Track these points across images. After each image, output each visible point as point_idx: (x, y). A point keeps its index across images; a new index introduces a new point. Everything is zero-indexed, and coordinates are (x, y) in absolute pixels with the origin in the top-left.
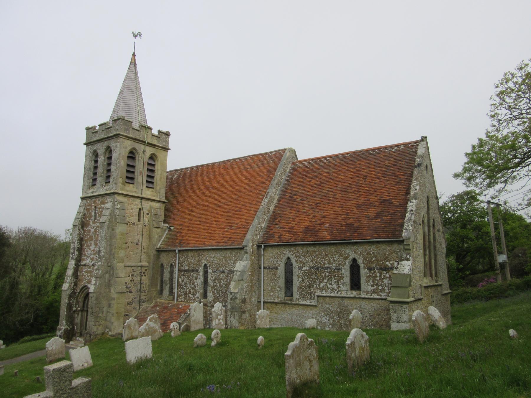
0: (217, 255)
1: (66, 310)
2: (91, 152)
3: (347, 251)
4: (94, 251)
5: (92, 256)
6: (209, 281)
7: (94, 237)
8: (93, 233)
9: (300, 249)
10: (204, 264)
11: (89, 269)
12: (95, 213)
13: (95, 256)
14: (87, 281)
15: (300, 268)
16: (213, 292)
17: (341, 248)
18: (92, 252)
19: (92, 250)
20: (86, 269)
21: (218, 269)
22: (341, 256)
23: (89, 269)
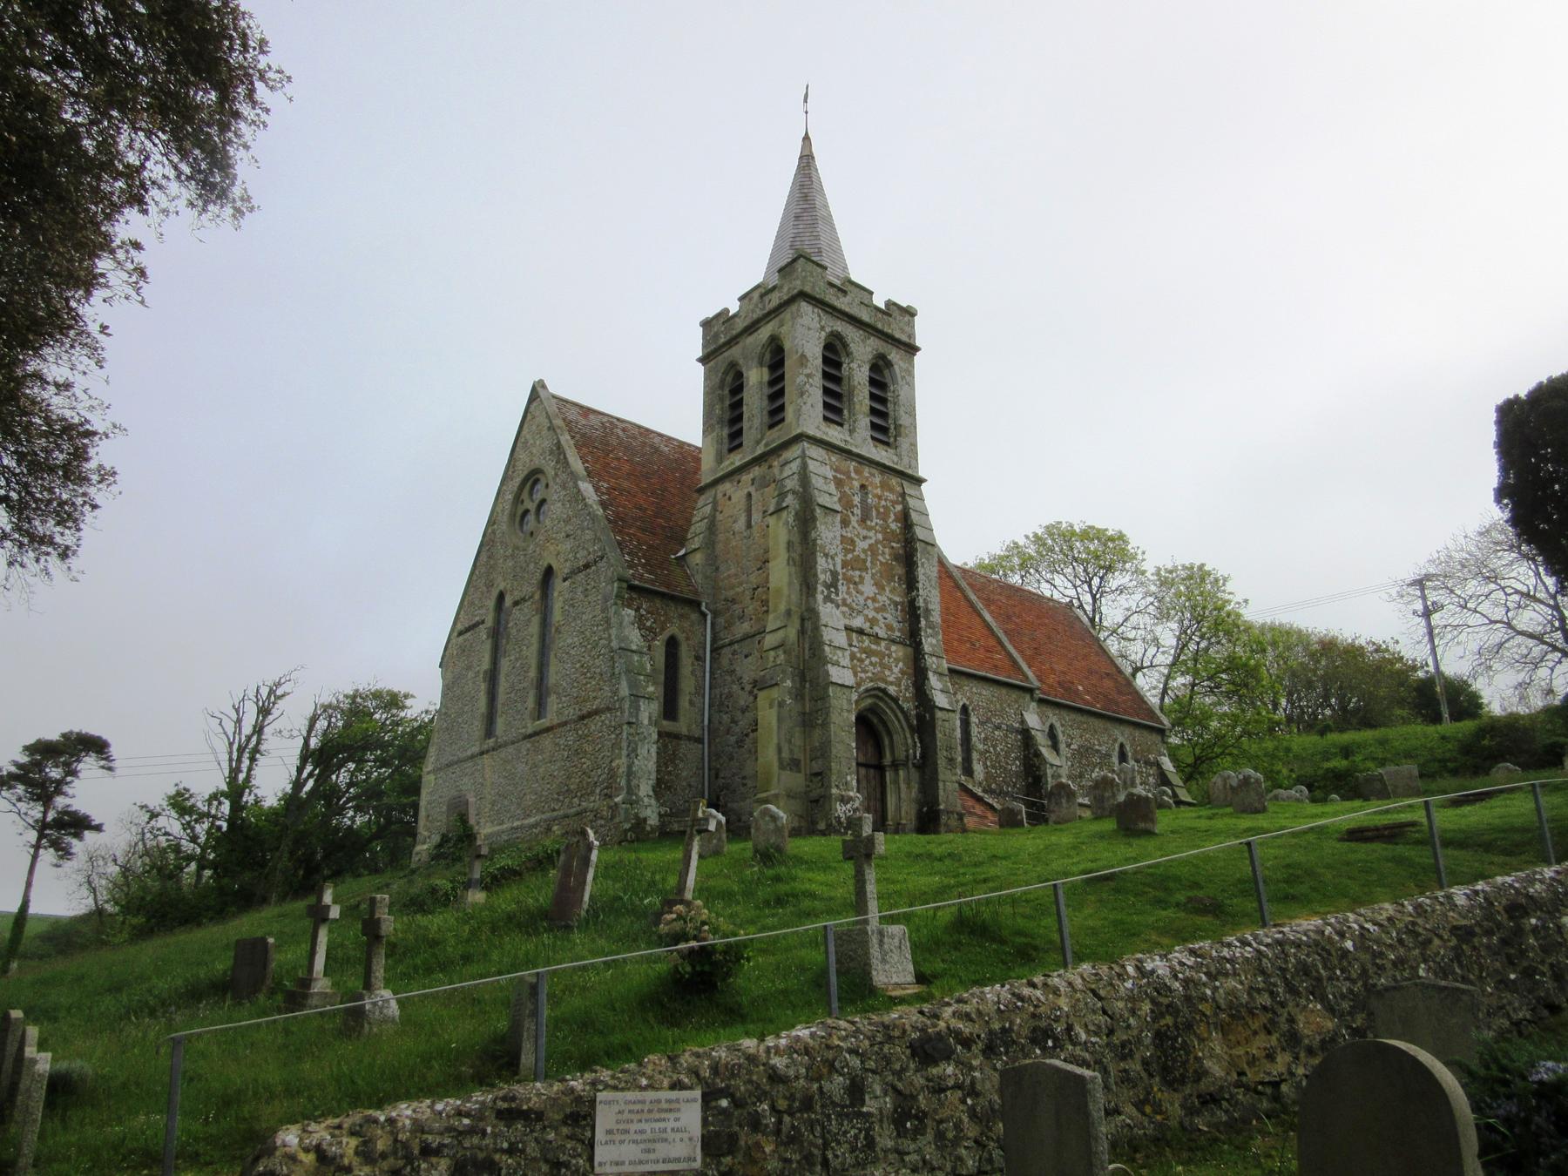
0: (986, 691)
1: (854, 745)
2: (822, 328)
3: (1116, 732)
4: (874, 600)
5: (871, 614)
6: (974, 739)
7: (868, 564)
8: (864, 551)
9: (1064, 713)
10: (961, 704)
11: (874, 647)
12: (863, 502)
13: (879, 617)
14: (870, 674)
15: (1069, 746)
16: (984, 764)
17: (1109, 725)
18: (869, 602)
19: (868, 598)
20: (863, 642)
21: (989, 720)
22: (1110, 736)
23: (874, 647)
